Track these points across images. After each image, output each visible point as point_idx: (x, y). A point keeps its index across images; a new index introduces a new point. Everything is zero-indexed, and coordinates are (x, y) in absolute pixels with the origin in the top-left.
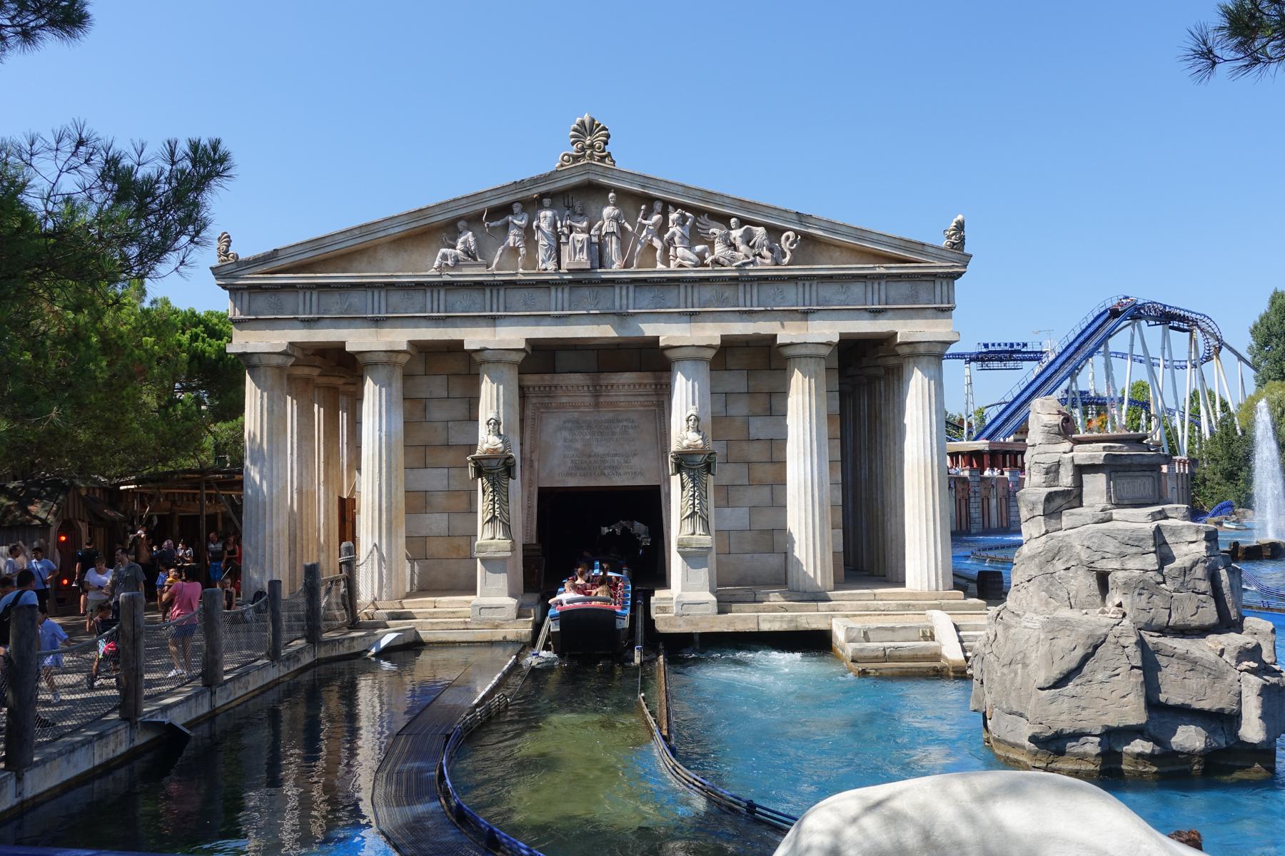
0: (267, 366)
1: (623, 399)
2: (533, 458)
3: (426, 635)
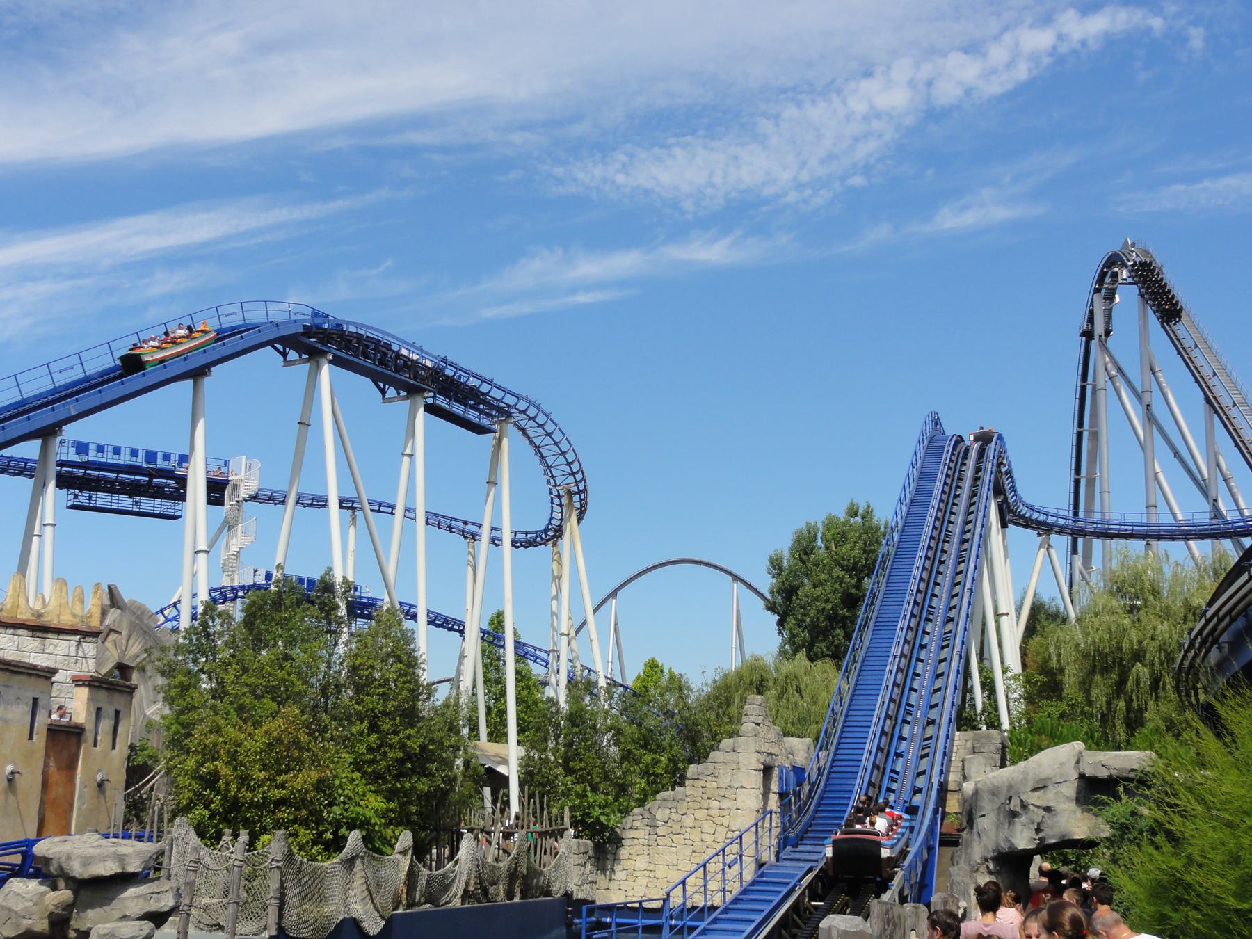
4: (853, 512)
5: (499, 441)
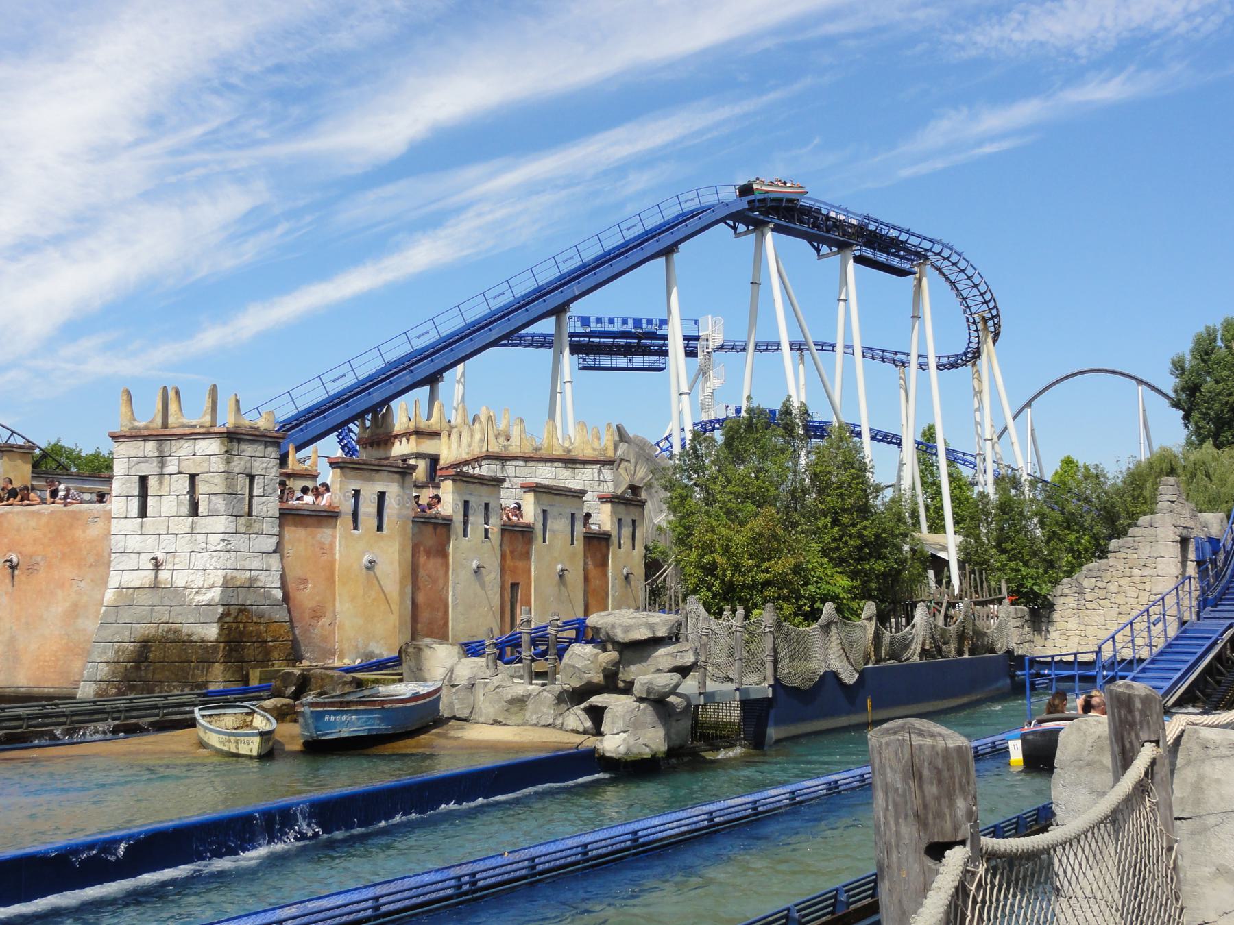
5: (920, 281)
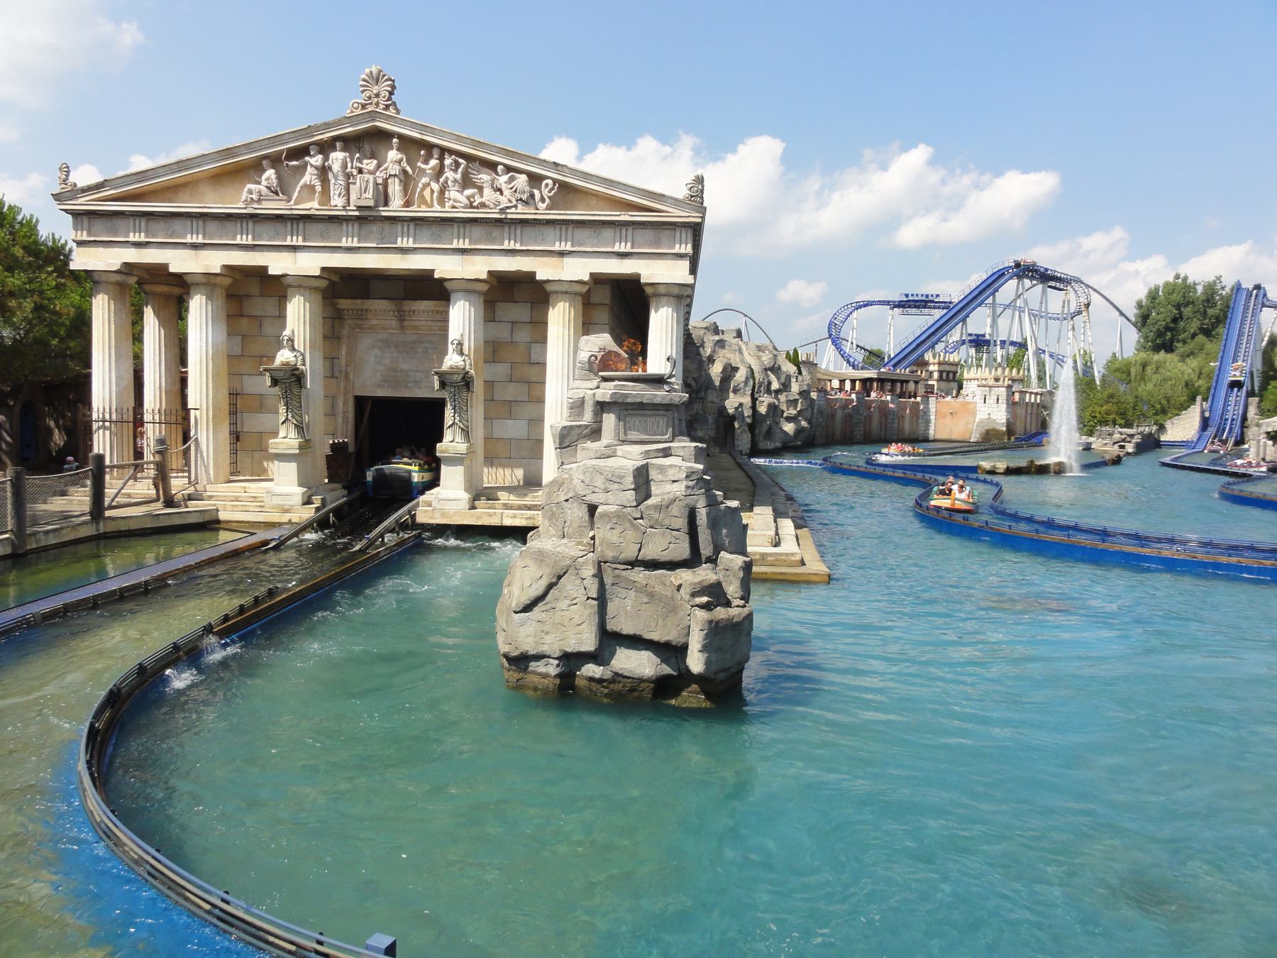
0: (108, 283)
1: (424, 323)
2: (349, 369)
3: (223, 516)
4: (1177, 277)
